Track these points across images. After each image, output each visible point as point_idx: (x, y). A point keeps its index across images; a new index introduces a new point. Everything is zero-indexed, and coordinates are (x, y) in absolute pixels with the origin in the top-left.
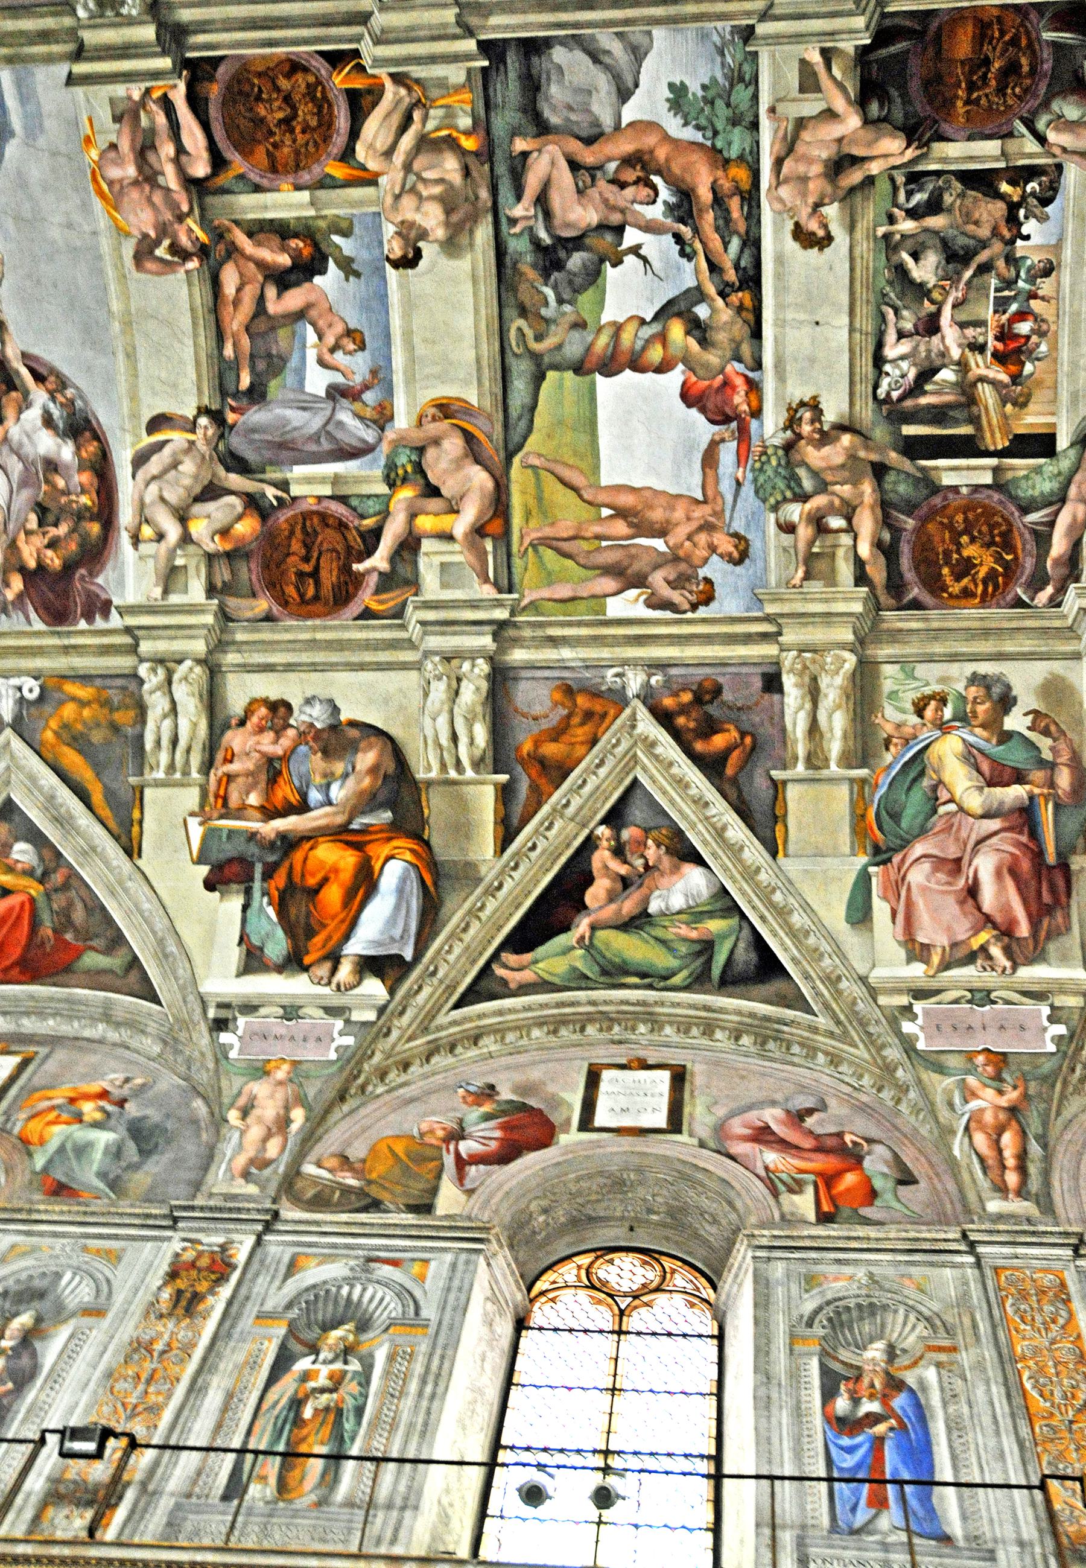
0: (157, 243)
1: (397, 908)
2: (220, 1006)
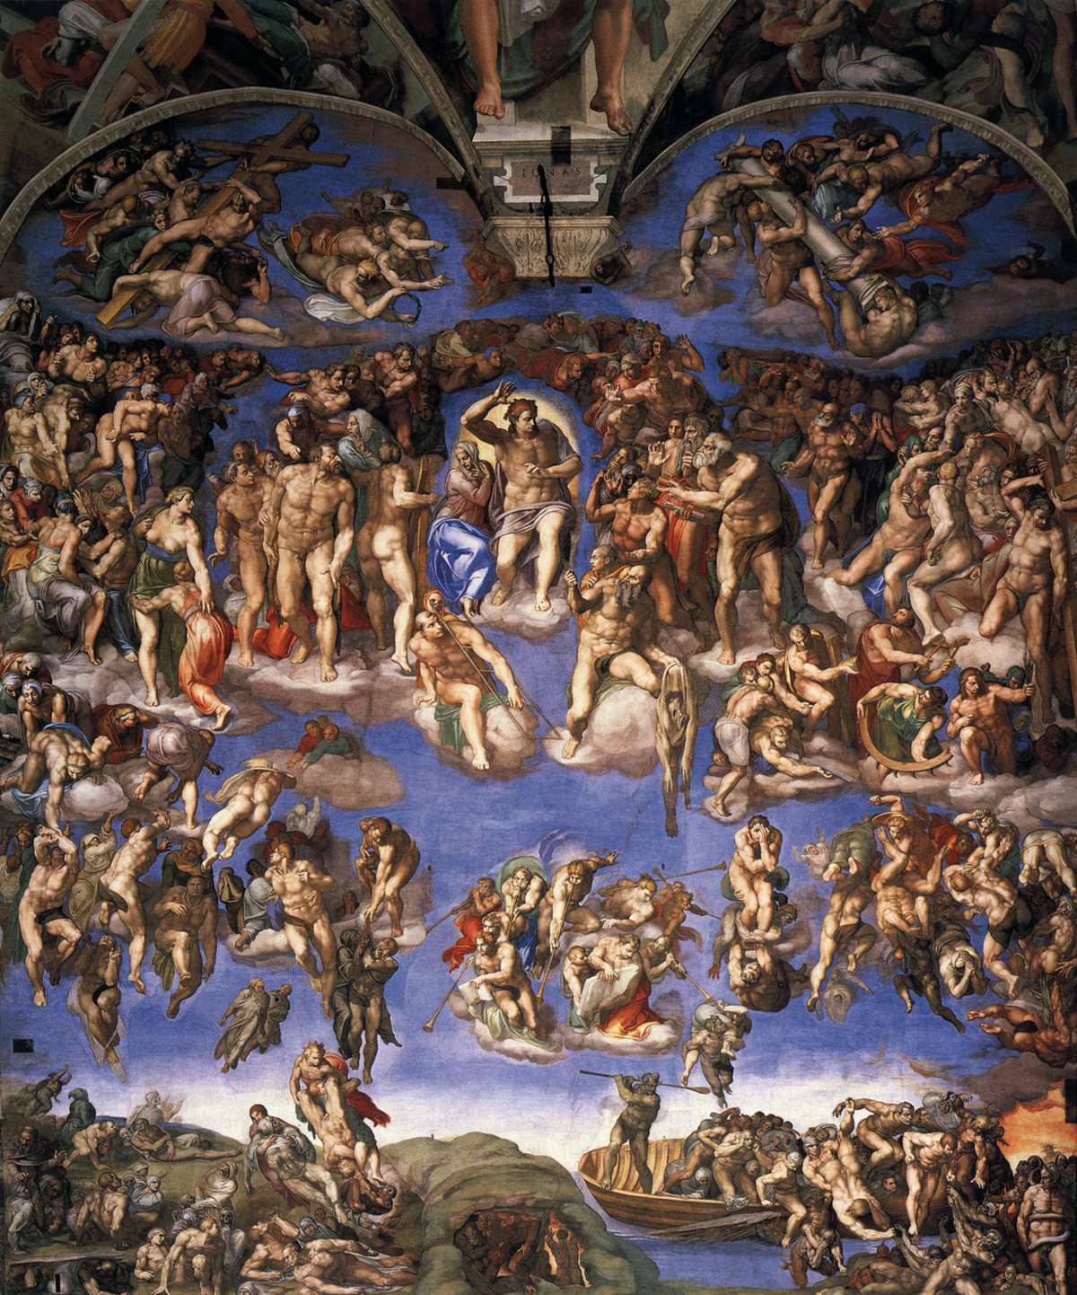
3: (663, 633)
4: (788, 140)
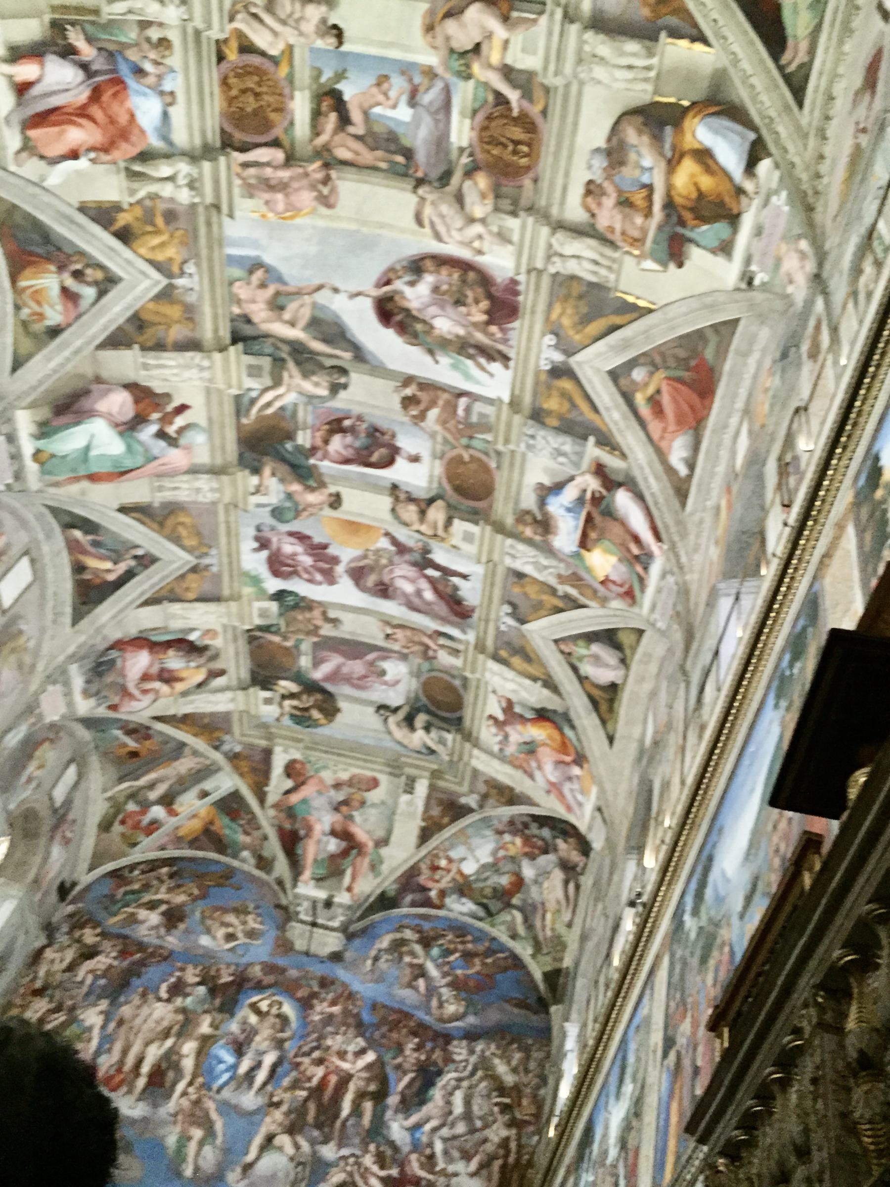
0: (320, 192)
1: (725, 136)
2: (742, 279)
3: (307, 1128)
4: (427, 926)
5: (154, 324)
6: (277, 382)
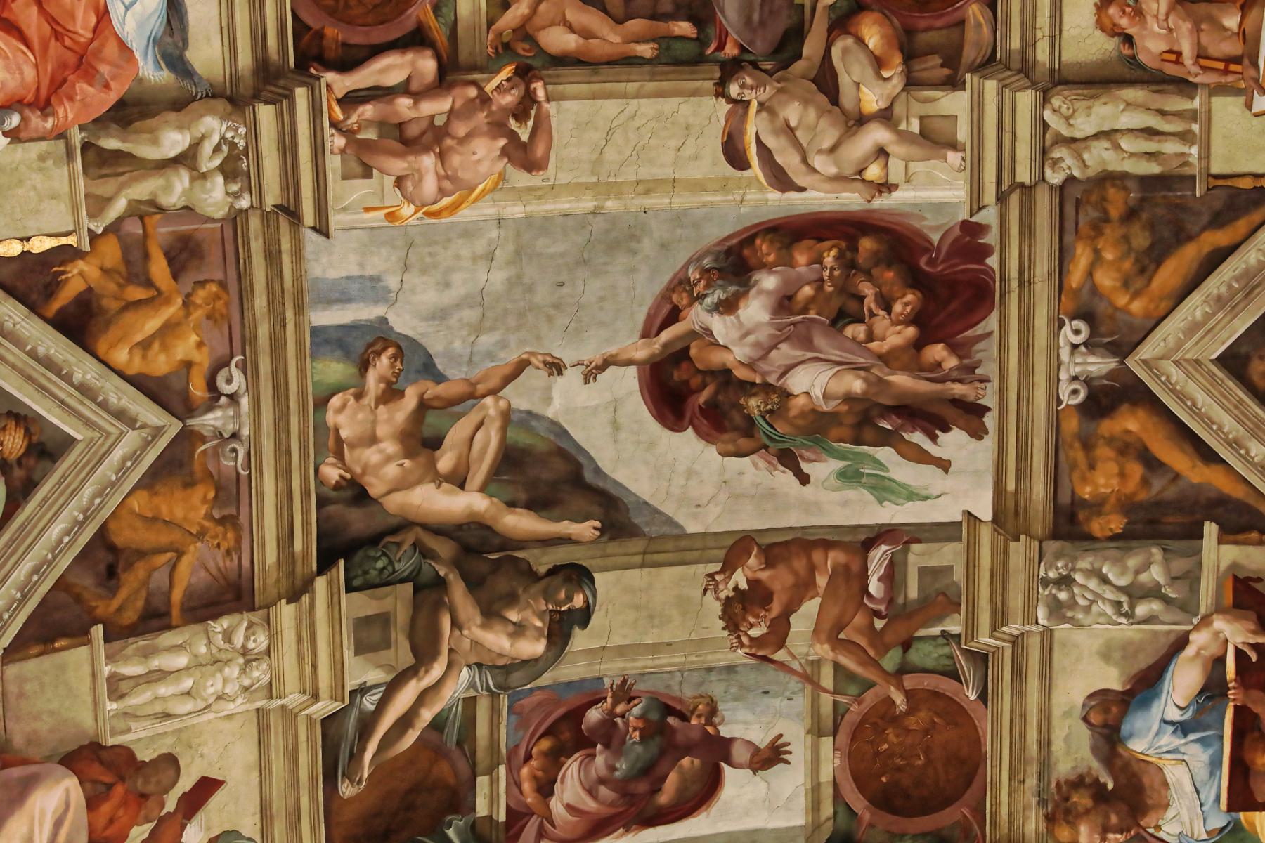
0: (513, 136)
5: (142, 554)
6: (424, 653)
